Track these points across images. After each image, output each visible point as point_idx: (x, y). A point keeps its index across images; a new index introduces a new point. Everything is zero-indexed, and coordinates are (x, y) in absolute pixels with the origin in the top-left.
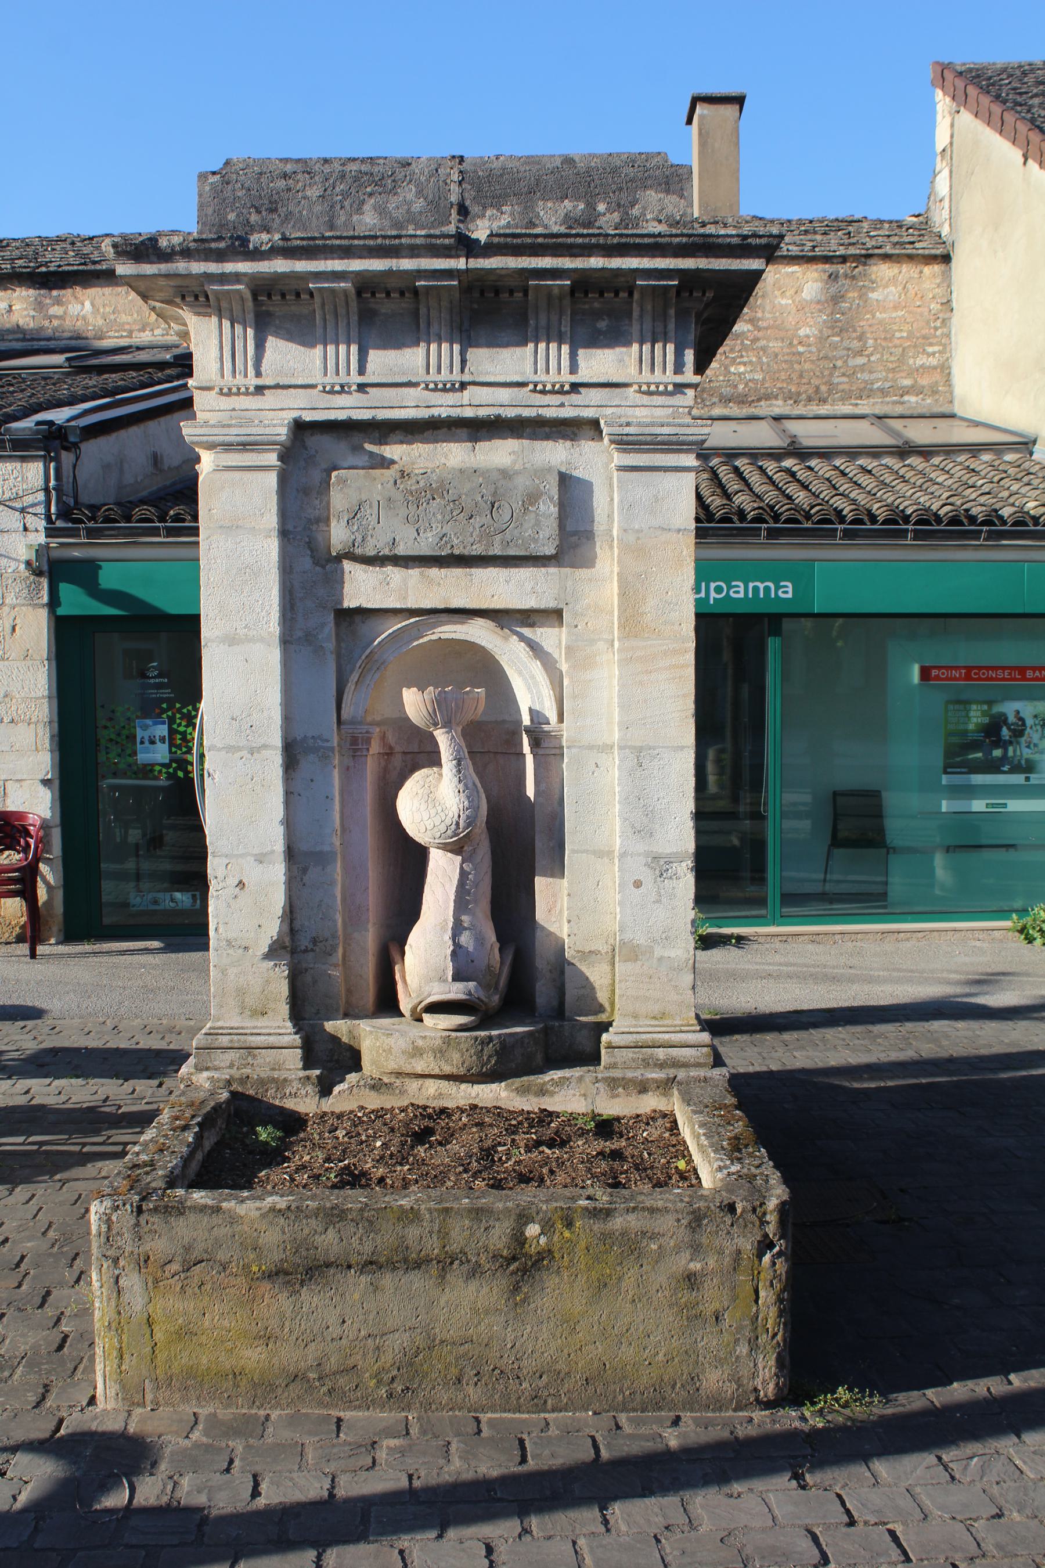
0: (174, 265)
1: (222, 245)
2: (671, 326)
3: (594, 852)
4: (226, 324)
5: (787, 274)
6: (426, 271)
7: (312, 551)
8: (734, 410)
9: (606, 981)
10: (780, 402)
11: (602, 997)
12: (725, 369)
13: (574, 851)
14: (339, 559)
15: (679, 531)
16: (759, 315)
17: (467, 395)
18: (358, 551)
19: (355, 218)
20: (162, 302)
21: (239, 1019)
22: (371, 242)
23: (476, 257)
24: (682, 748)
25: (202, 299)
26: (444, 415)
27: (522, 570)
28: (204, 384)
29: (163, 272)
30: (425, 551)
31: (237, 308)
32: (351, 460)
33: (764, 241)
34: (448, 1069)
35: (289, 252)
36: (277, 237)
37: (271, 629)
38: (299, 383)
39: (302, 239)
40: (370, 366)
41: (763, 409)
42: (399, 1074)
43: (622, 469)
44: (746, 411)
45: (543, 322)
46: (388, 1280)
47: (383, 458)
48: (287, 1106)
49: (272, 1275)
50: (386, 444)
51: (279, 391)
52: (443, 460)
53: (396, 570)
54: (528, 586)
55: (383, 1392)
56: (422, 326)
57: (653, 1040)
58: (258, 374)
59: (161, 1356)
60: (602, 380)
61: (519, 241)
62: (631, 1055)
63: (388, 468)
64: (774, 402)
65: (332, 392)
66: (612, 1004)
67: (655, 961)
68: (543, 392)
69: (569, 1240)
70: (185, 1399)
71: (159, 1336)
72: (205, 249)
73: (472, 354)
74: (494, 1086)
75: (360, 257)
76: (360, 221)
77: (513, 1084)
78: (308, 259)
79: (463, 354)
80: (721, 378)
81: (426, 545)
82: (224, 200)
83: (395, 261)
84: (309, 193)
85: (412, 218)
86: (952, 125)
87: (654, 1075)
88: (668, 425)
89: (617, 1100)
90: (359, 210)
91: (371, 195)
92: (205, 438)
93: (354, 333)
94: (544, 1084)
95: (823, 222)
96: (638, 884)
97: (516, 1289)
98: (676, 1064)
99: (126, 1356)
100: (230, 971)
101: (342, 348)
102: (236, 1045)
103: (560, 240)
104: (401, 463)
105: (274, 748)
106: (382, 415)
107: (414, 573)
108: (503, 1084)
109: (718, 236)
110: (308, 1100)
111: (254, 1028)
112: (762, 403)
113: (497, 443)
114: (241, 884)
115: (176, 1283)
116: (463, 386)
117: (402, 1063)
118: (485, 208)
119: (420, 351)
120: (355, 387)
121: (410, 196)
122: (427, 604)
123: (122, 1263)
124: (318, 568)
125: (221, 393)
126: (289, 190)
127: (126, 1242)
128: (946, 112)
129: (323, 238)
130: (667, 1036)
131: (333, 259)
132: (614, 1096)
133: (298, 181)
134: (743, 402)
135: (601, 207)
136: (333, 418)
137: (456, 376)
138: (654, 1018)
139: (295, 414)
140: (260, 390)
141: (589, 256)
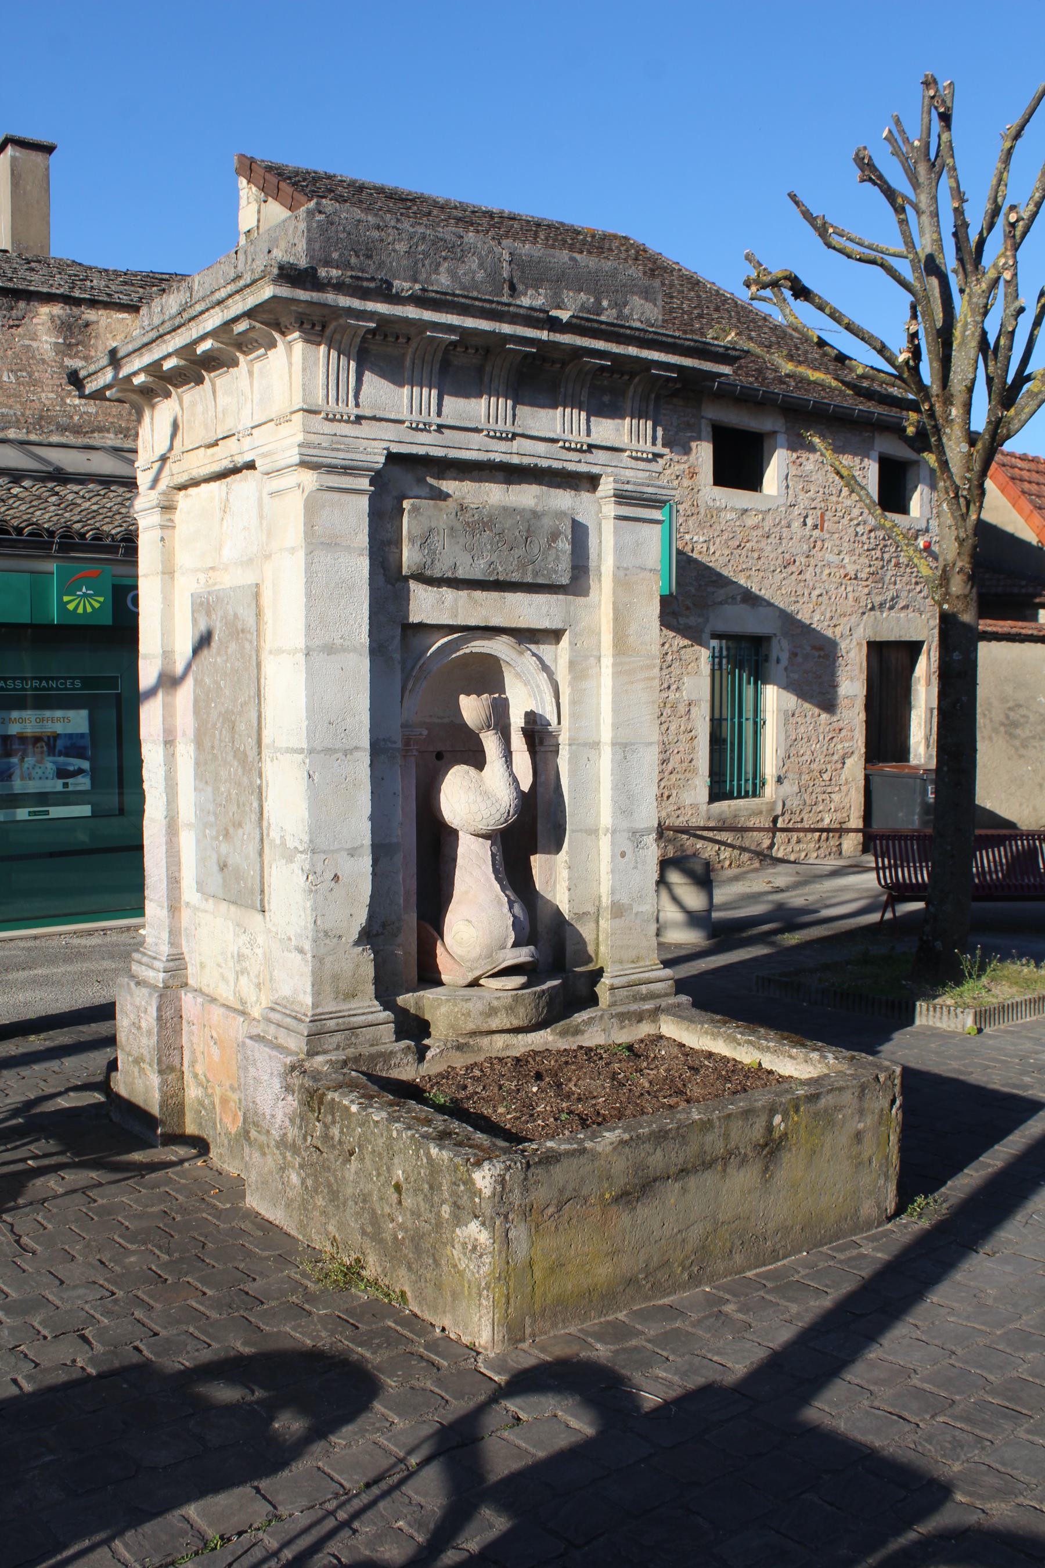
0: (325, 295)
1: (372, 285)
2: (651, 407)
3: (586, 831)
4: (334, 354)
5: (118, 319)
6: (518, 337)
7: (384, 568)
8: (69, 438)
10: (111, 436)
11: (591, 949)
13: (573, 831)
14: (406, 579)
15: (651, 570)
16: (93, 353)
18: (428, 573)
19: (434, 277)
20: (262, 323)
21: (334, 1003)
22: (488, 306)
23: (555, 331)
24: (651, 744)
27: (540, 596)
28: (314, 408)
29: (315, 300)
30: (479, 576)
33: (737, 353)
34: (516, 1023)
35: (421, 301)
36: (417, 286)
38: (392, 417)
39: (437, 292)
40: (445, 410)
42: (473, 1034)
44: (81, 441)
45: (570, 391)
46: (692, 1181)
47: (441, 491)
48: (392, 1076)
49: (616, 1200)
50: (444, 479)
51: (374, 422)
52: (485, 498)
53: (449, 590)
54: (544, 610)
55: (686, 1276)
56: (486, 379)
57: (639, 980)
58: (357, 405)
59: (538, 1292)
60: (609, 444)
61: (589, 324)
62: (625, 993)
63: (445, 500)
64: (107, 435)
65: (417, 429)
66: (597, 954)
67: (633, 916)
68: (569, 449)
69: (797, 1123)
70: (554, 1325)
71: (538, 1274)
73: (521, 410)
74: (542, 1032)
75: (473, 317)
76: (437, 280)
77: (556, 1028)
78: (432, 310)
79: (514, 408)
80: (58, 408)
81: (477, 570)
82: (329, 239)
83: (498, 324)
84: (397, 247)
85: (475, 286)
86: (259, 212)
87: (647, 1007)
88: (652, 486)
89: (625, 1030)
91: (445, 259)
92: (315, 459)
93: (435, 380)
94: (579, 1024)
95: (136, 276)
96: (623, 855)
97: (767, 1168)
98: (652, 996)
99: (512, 1301)
101: (425, 391)
102: (342, 1027)
103: (616, 329)
104: (455, 497)
106: (453, 454)
107: (463, 594)
108: (549, 1030)
110: (408, 1068)
111: (349, 1010)
112: (96, 435)
113: (525, 487)
115: (551, 1224)
116: (515, 435)
119: (484, 401)
120: (434, 427)
121: (474, 266)
122: (472, 622)
123: (511, 1217)
124: (389, 586)
125: (327, 419)
126: (382, 241)
127: (516, 1197)
128: (251, 199)
129: (454, 295)
130: (646, 975)
131: (452, 314)
133: (389, 235)
134: (78, 433)
135: (605, 303)
136: (414, 452)
137: (509, 427)
138: (633, 962)
139: (385, 445)
140: (359, 419)
141: (628, 345)
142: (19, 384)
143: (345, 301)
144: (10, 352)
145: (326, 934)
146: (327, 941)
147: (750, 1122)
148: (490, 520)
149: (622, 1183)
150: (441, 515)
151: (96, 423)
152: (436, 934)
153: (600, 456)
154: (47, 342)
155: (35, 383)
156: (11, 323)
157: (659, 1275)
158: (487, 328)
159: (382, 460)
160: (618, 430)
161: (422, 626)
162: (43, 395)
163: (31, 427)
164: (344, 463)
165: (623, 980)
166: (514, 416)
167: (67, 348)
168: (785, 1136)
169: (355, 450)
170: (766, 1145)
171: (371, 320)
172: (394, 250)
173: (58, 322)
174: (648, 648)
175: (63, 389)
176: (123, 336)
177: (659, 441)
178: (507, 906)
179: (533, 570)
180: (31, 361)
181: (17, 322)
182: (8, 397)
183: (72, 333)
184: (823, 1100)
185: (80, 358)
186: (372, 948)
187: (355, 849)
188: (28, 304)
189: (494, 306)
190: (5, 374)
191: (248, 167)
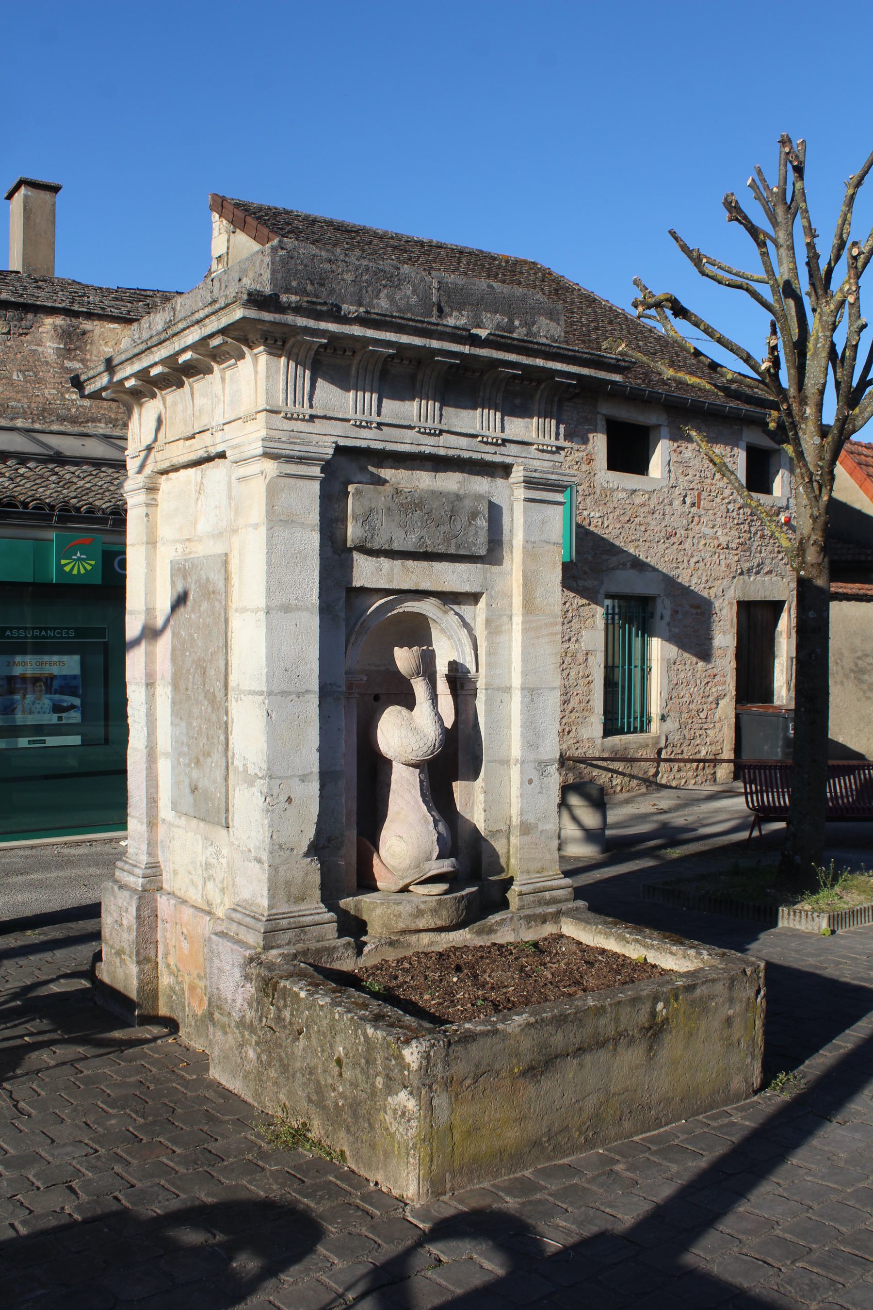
0: (286, 316)
1: (325, 308)
2: (555, 408)
4: (292, 364)
8: (67, 427)
9: (505, 850)
10: (103, 425)
11: (503, 861)
12: (62, 395)
13: (488, 762)
14: (351, 550)
16: (88, 357)
17: (444, 439)
18: (369, 545)
19: (375, 301)
20: (233, 339)
21: (287, 905)
22: (420, 325)
23: (475, 347)
24: (554, 688)
25: (279, 343)
26: (427, 452)
30: (411, 548)
31: (302, 354)
32: (359, 477)
33: (626, 364)
34: (440, 923)
35: (364, 321)
36: (362, 310)
37: (313, 601)
39: (378, 314)
41: (90, 428)
42: (404, 932)
43: (527, 500)
44: (77, 429)
46: (588, 1058)
47: (380, 477)
48: (335, 967)
49: (523, 1074)
51: (325, 421)
53: (386, 560)
54: (465, 576)
55: (582, 1139)
57: (544, 887)
58: (311, 406)
59: (457, 1152)
60: (519, 439)
61: (504, 340)
63: (383, 485)
65: (360, 426)
66: (508, 865)
67: (539, 834)
68: (487, 443)
69: (677, 1009)
70: (470, 1181)
71: (457, 1137)
72: (312, 309)
73: (448, 411)
76: (378, 304)
77: (473, 928)
78: (374, 329)
79: (441, 409)
80: (58, 402)
81: (409, 543)
82: (289, 270)
83: (428, 340)
84: (345, 277)
86: (228, 241)
87: (550, 910)
88: (556, 473)
89: (531, 930)
90: (377, 297)
91: (385, 286)
92: (276, 451)
94: (492, 925)
95: (125, 293)
96: (530, 782)
97: (651, 1048)
98: (554, 901)
99: (435, 1159)
100: (280, 869)
101: (368, 395)
102: (293, 926)
105: (314, 692)
106: (390, 447)
107: (398, 563)
108: (467, 929)
109: (607, 357)
110: (348, 961)
112: (89, 424)
113: (450, 474)
114: (289, 800)
115: (468, 1094)
116: (441, 432)
117: (409, 923)
118: (452, 311)
119: (416, 403)
120: (374, 425)
121: (409, 293)
122: (405, 586)
124: (336, 556)
125: (286, 418)
126: (333, 272)
128: (222, 231)
129: (392, 316)
131: (390, 332)
132: (529, 928)
133: (339, 267)
134: (75, 422)
135: (517, 323)
137: (437, 425)
138: (538, 872)
139: (334, 439)
140: (312, 418)
141: (536, 357)
142: (26, 382)
143: (302, 321)
144: (19, 356)
145: (281, 847)
146: (282, 853)
147: (637, 1008)
148: (421, 502)
149: (528, 1059)
150: (379, 498)
151: (90, 415)
152: (373, 848)
153: (512, 449)
154: (50, 347)
155: (40, 381)
156: (21, 331)
157: (560, 1139)
158: (419, 344)
159: (331, 451)
160: (527, 427)
161: (363, 590)
162: (46, 391)
163: (36, 418)
164: (299, 454)
165: (530, 888)
166: (441, 415)
167: (67, 353)
168: (666, 1020)
169: (309, 443)
170: (651, 1028)
171: (323, 337)
172: (343, 280)
173: (60, 331)
174: (552, 608)
175: (63, 387)
176: (114, 342)
177: (562, 436)
178: (432, 824)
179: (456, 543)
180: (37, 363)
181: (25, 331)
182: (17, 392)
183: (71, 340)
184: (699, 991)
185: (77, 360)
186: (319, 859)
187: (305, 775)
188: (35, 316)
189: (425, 325)
190: (15, 373)
191: (220, 204)
